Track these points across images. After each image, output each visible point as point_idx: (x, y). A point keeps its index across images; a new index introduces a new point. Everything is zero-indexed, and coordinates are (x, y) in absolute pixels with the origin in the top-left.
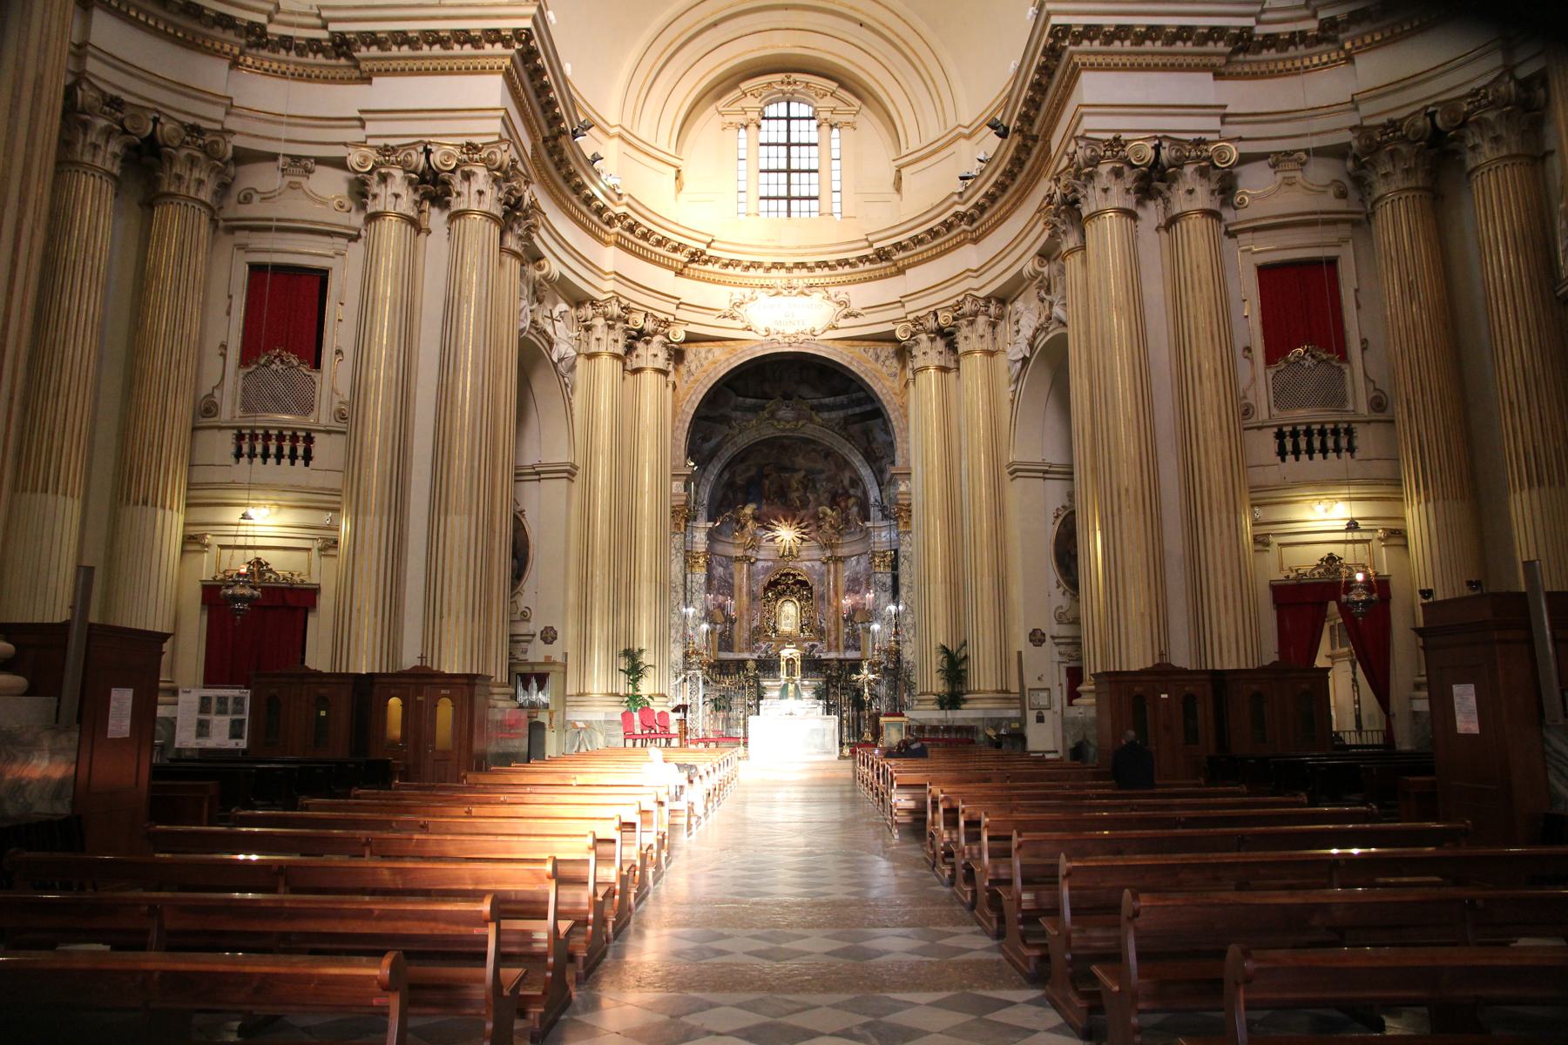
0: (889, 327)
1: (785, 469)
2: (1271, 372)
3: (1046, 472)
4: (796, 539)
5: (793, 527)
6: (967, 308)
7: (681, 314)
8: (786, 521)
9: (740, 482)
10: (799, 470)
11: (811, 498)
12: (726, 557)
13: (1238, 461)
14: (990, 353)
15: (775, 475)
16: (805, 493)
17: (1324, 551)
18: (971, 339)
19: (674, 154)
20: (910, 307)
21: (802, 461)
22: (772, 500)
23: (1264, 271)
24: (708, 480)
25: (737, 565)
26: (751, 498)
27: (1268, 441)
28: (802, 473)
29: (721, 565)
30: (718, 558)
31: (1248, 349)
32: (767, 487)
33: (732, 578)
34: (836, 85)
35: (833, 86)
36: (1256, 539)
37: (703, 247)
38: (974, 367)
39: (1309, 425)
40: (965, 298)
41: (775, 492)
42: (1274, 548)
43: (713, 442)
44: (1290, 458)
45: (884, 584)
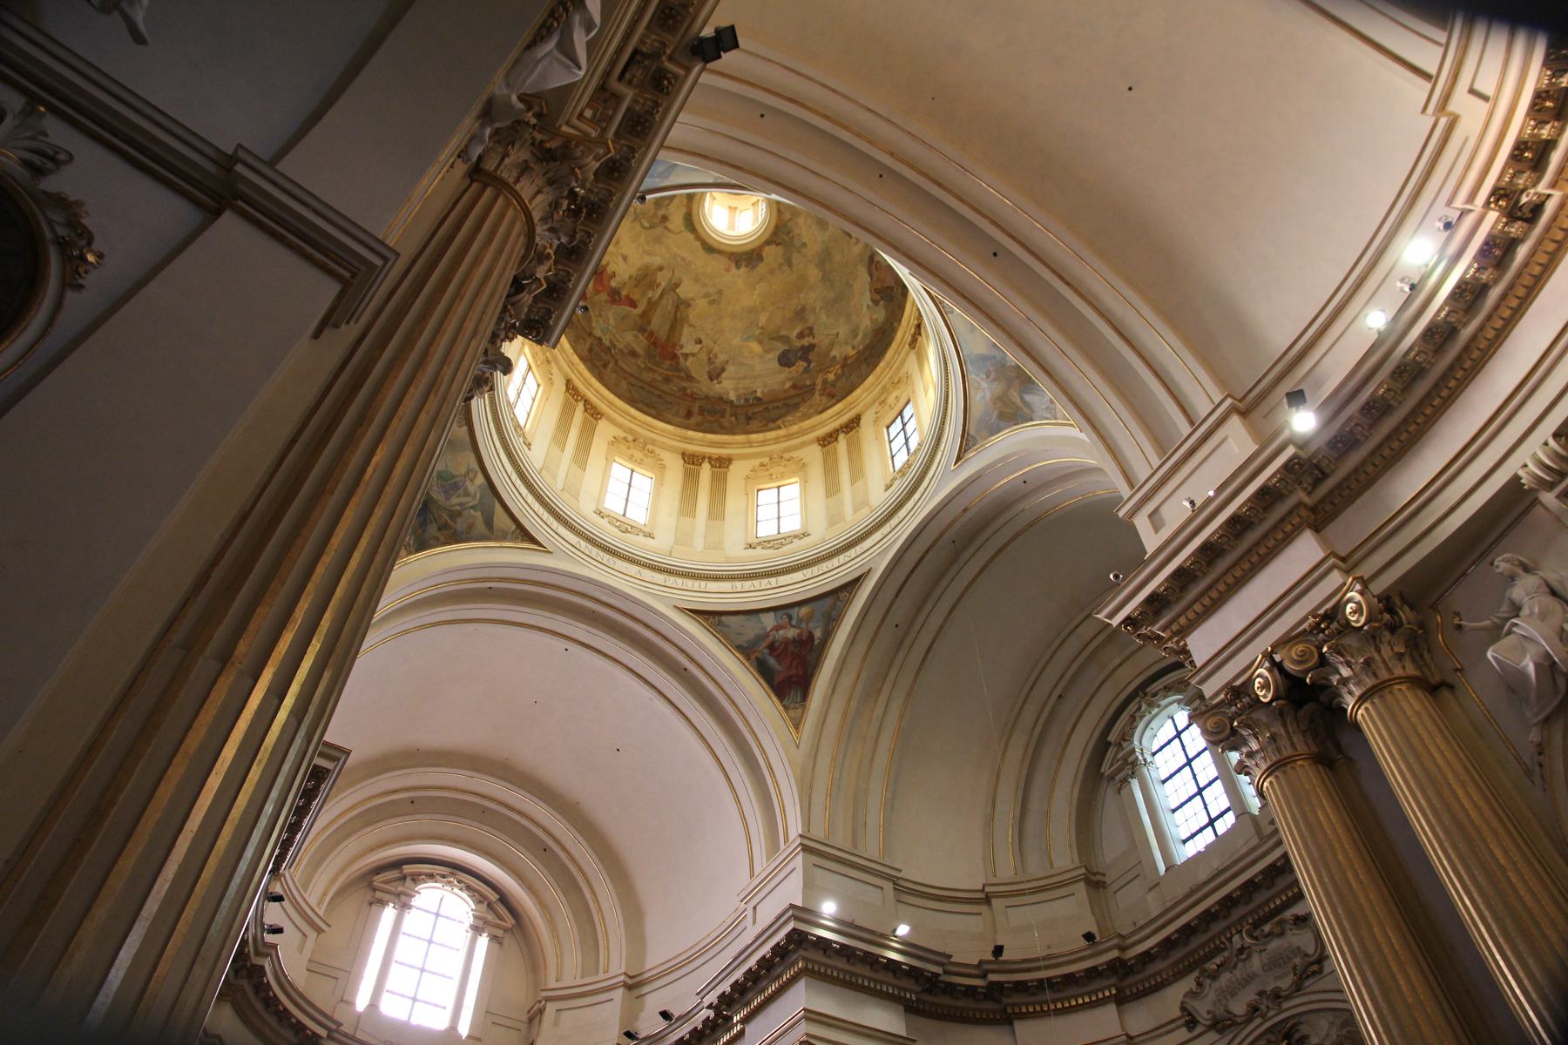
19: (321, 913)
34: (498, 897)
35: (493, 896)
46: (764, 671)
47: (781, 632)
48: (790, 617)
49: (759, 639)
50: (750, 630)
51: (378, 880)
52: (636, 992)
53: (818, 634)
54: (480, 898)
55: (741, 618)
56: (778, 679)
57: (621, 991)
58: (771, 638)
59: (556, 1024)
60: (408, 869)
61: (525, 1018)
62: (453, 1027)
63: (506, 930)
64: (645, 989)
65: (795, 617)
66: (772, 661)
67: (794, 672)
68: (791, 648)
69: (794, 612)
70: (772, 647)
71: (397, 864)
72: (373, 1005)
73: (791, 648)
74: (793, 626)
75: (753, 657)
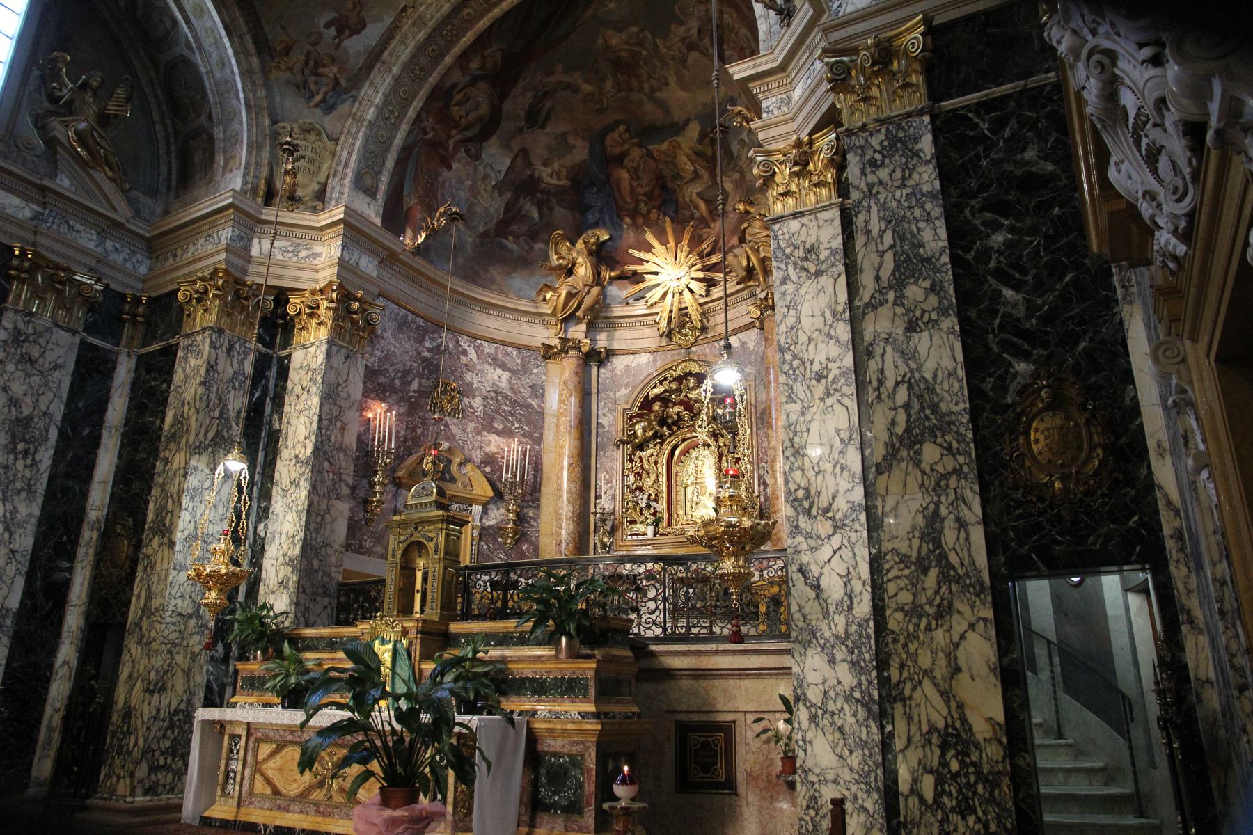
1: (648, 132)
4: (695, 286)
5: (681, 256)
8: (664, 243)
9: (554, 181)
10: (687, 122)
11: (729, 186)
12: (519, 347)
15: (636, 153)
16: (713, 175)
21: (683, 95)
22: (646, 217)
24: (360, 121)
25: (553, 365)
26: (590, 218)
28: (694, 130)
29: (503, 366)
30: (489, 348)
32: (625, 186)
33: (542, 396)
41: (649, 196)
43: (372, 33)
45: (812, 250)
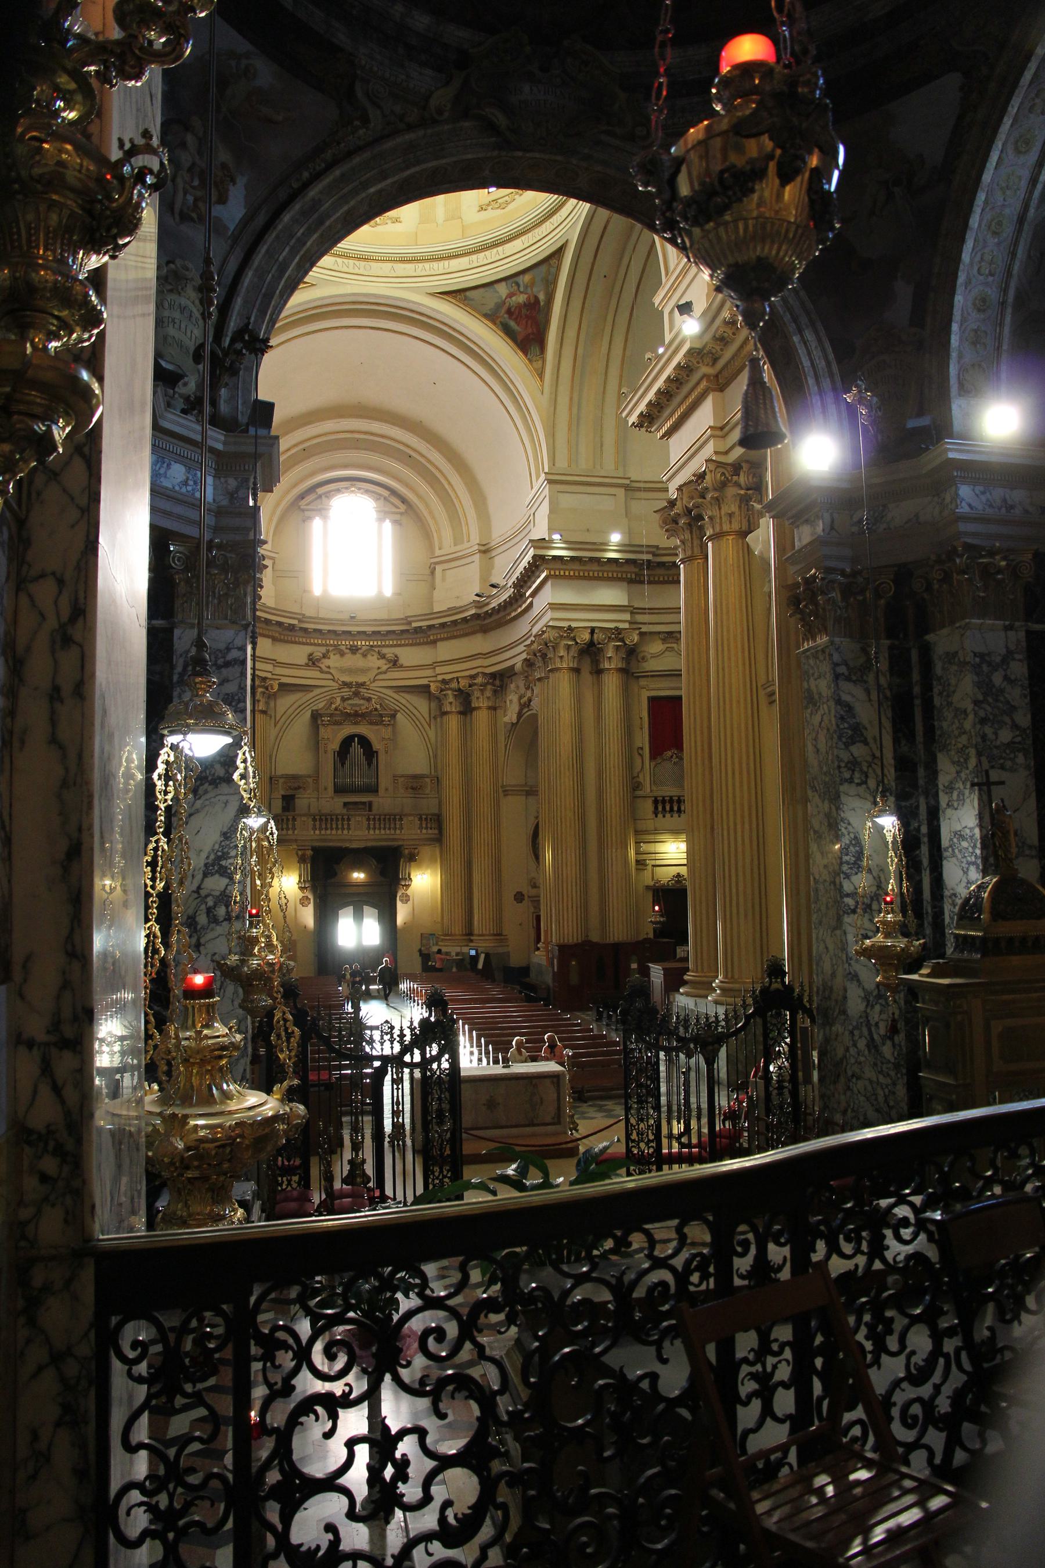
0: (425, 682)
2: (653, 764)
3: (527, 791)
6: (479, 680)
7: (279, 671)
13: (632, 814)
14: (493, 708)
17: (674, 871)
18: (481, 701)
20: (438, 670)
23: (653, 701)
27: (649, 805)
31: (642, 748)
35: (386, 493)
36: (638, 862)
37: (295, 622)
38: (481, 718)
39: (671, 797)
40: (477, 675)
42: (649, 868)
44: (660, 816)
46: (508, 332)
47: (514, 298)
48: (518, 285)
49: (499, 306)
50: (490, 299)
51: (303, 503)
52: (489, 555)
53: (542, 297)
54: (377, 497)
55: (481, 290)
56: (520, 338)
57: (478, 556)
58: (507, 305)
59: (444, 579)
60: (320, 491)
61: (428, 572)
62: (380, 592)
63: (401, 514)
64: (494, 553)
65: (521, 283)
66: (512, 324)
67: (530, 331)
68: (524, 311)
69: (520, 279)
70: (509, 312)
71: (312, 489)
72: (325, 591)
73: (524, 311)
74: (521, 293)
75: (498, 322)
